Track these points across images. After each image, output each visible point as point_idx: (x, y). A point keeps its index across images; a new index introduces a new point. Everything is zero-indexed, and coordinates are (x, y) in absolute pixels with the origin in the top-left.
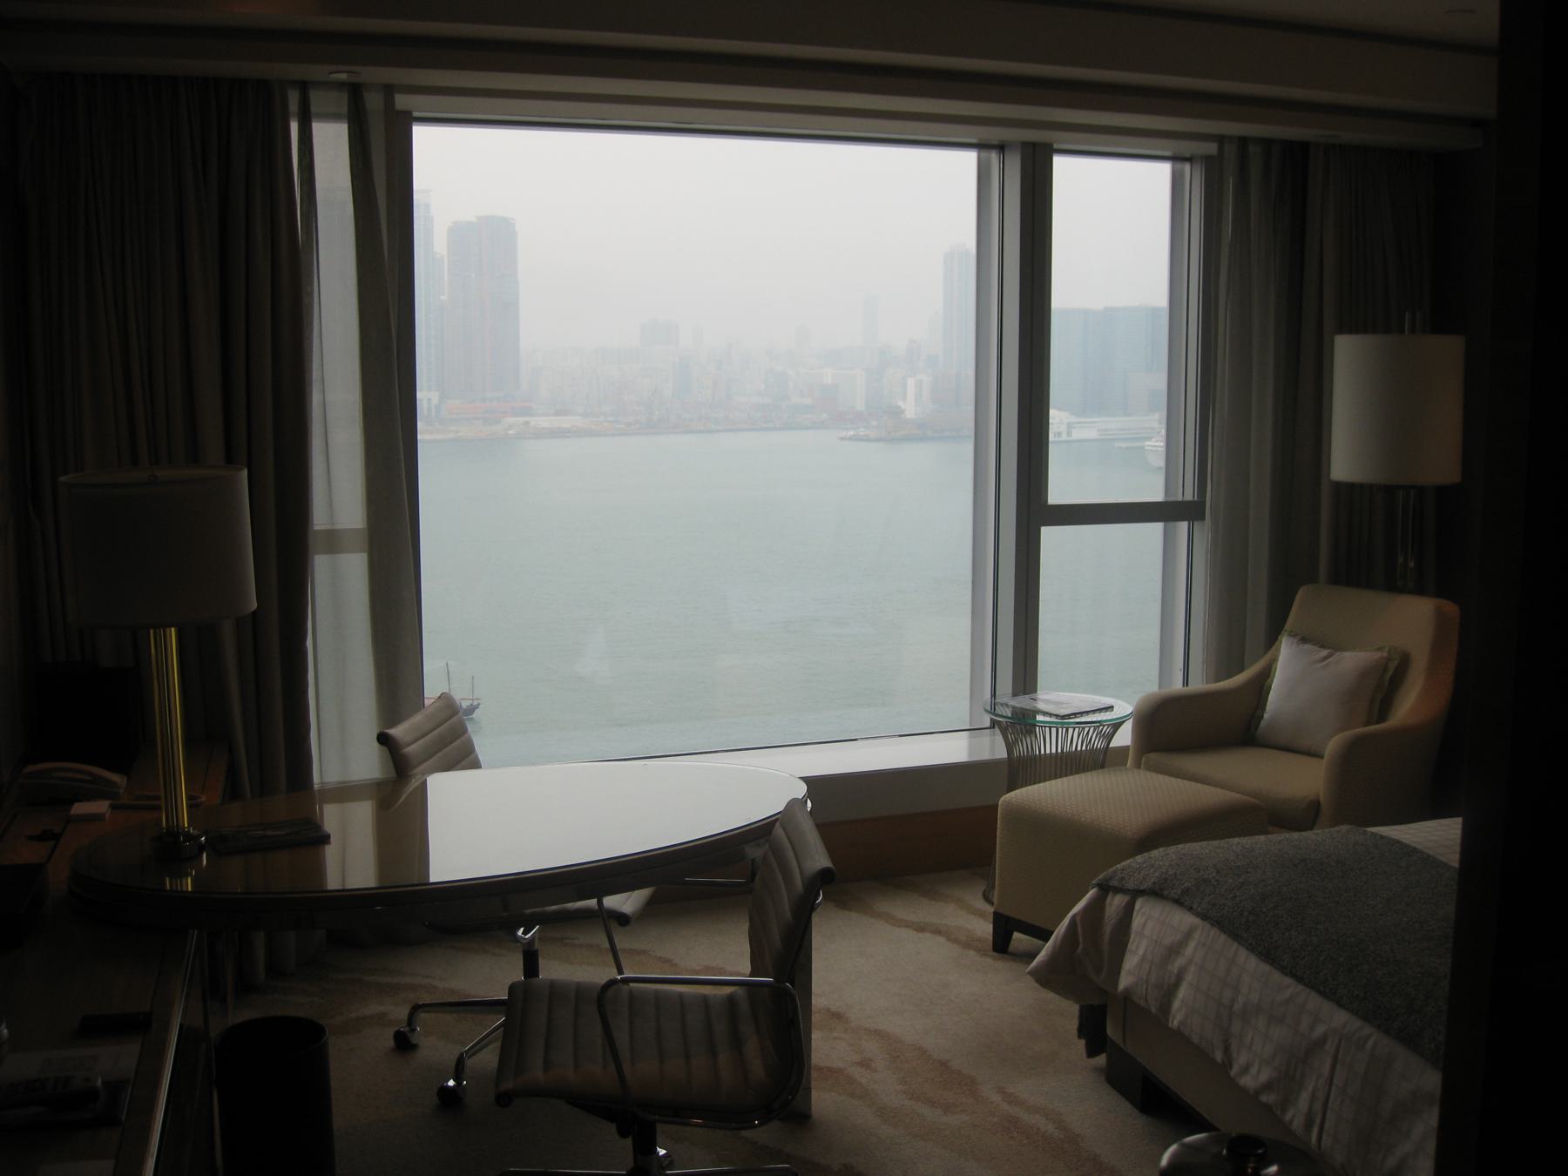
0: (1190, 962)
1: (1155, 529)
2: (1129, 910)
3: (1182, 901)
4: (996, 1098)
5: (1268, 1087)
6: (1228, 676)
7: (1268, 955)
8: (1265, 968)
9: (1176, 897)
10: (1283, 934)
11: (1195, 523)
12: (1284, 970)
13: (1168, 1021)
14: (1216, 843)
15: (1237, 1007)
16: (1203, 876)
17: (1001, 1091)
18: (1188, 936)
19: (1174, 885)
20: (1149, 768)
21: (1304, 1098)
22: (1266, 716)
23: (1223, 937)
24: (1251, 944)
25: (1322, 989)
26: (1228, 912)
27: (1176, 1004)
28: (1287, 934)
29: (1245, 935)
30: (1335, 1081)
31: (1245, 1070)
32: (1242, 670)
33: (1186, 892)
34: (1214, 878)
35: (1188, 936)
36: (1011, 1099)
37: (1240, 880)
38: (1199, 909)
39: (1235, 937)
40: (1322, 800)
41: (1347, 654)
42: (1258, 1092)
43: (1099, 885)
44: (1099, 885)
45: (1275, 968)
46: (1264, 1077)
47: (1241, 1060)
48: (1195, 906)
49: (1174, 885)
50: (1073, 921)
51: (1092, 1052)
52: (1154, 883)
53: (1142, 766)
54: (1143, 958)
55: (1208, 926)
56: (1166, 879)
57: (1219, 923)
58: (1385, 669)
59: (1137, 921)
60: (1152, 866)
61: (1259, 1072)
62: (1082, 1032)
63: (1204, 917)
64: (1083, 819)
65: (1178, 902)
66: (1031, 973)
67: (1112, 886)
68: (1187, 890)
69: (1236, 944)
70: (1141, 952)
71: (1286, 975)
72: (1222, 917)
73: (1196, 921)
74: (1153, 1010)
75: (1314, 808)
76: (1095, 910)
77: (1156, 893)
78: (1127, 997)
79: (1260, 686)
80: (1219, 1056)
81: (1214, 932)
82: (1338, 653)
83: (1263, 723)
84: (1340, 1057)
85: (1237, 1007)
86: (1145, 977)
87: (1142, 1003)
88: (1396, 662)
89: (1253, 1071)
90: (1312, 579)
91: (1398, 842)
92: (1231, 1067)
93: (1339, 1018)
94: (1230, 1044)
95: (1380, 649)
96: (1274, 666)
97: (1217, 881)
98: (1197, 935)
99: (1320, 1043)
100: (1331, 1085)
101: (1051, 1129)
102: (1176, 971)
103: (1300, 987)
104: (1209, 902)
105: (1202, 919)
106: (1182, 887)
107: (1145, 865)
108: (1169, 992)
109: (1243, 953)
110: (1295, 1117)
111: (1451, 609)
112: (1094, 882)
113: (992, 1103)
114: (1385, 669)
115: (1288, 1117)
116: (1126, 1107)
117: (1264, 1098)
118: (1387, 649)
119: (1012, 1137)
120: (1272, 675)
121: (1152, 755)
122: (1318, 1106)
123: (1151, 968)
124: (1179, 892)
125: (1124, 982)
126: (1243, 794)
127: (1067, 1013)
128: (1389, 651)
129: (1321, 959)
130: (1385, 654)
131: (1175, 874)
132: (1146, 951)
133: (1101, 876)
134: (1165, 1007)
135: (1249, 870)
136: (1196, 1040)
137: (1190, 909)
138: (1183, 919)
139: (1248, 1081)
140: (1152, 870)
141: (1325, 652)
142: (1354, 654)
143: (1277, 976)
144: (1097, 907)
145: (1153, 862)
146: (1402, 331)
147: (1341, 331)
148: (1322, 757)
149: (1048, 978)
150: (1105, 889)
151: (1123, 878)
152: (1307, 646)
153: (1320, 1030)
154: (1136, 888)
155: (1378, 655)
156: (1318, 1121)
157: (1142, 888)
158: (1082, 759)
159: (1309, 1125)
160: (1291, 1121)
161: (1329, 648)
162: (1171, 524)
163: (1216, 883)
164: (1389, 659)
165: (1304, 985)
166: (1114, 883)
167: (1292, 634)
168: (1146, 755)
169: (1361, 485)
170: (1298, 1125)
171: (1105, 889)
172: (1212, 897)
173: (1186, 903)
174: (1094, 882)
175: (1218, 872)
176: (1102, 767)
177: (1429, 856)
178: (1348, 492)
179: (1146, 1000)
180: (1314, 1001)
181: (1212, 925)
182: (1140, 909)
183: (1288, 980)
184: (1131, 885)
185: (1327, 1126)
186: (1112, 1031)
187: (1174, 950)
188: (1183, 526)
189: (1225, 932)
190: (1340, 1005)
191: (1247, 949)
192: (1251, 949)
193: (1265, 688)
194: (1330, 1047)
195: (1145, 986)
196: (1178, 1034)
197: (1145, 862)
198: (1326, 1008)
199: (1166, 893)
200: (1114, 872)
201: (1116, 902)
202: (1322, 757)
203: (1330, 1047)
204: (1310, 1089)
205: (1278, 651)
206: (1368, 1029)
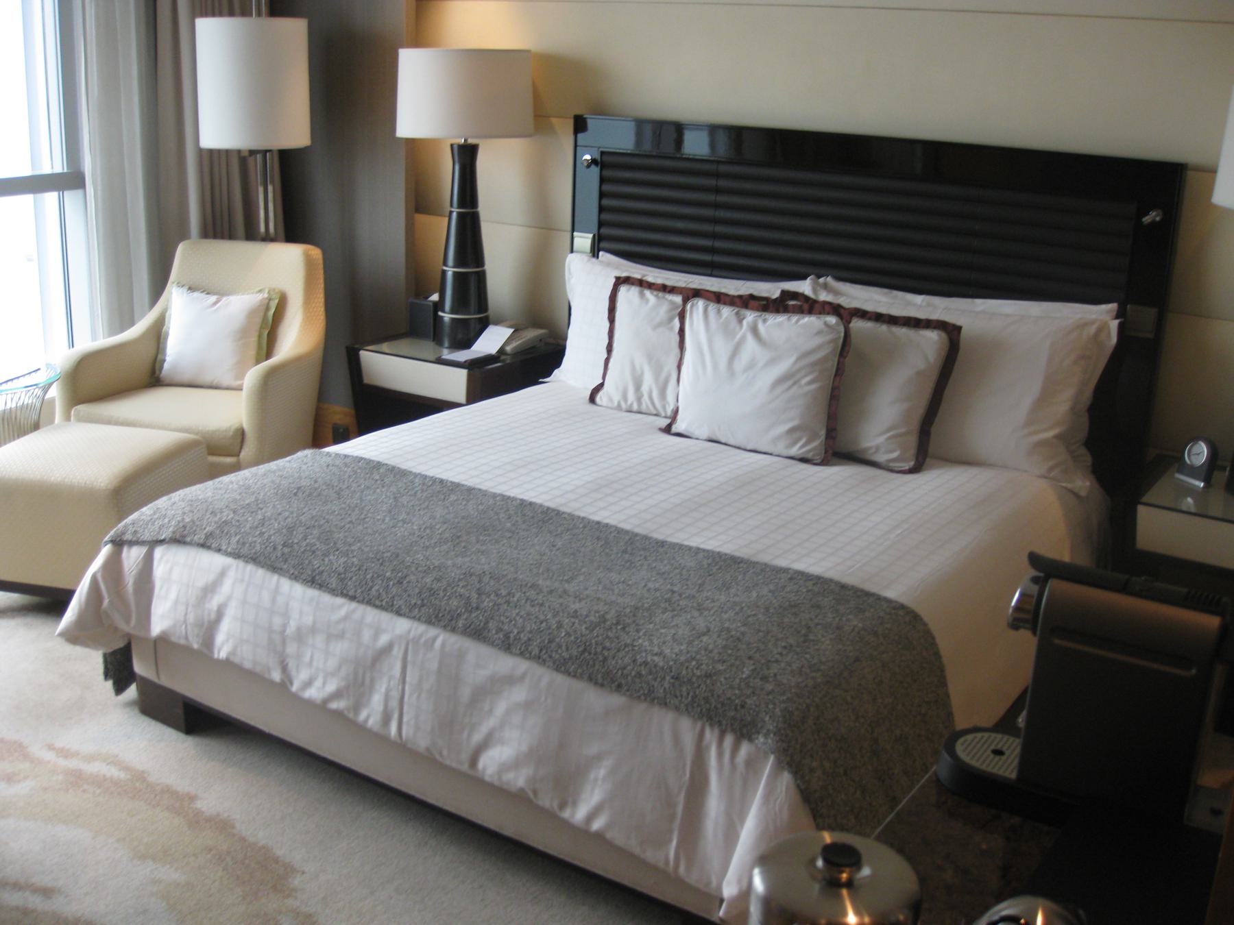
0: (229, 598)
1: (27, 199)
2: (148, 560)
3: (209, 544)
4: (49, 756)
5: (337, 695)
6: (122, 330)
7: (314, 581)
8: (312, 593)
9: (201, 541)
10: (323, 560)
11: (66, 193)
12: (333, 592)
13: (212, 652)
14: (210, 483)
15: (290, 630)
16: (220, 519)
17: (51, 747)
18: (222, 574)
19: (195, 531)
20: (81, 419)
21: (377, 701)
22: (168, 359)
23: (261, 572)
24: (293, 574)
25: (378, 603)
26: (261, 548)
27: (220, 638)
28: (326, 559)
29: (285, 567)
30: (408, 679)
31: (308, 684)
32: (132, 324)
33: (210, 535)
34: (233, 518)
35: (222, 574)
36: (65, 753)
37: (260, 517)
38: (229, 550)
39: (274, 568)
40: (245, 426)
41: (233, 298)
42: (326, 701)
43: (113, 541)
44: (113, 541)
45: (325, 591)
46: (331, 687)
47: (299, 678)
48: (224, 548)
49: (195, 531)
50: (94, 580)
51: (120, 688)
52: (174, 532)
53: (72, 418)
54: (176, 602)
55: (241, 564)
56: (184, 527)
57: (254, 559)
58: (268, 308)
59: (159, 570)
60: (165, 516)
61: (324, 683)
62: (107, 675)
63: (236, 555)
64: (53, 478)
65: (204, 546)
66: (62, 635)
67: (126, 541)
68: (211, 534)
69: (276, 577)
70: (173, 596)
71: (337, 596)
72: (255, 553)
73: (229, 561)
74: (196, 646)
75: (241, 434)
76: (113, 567)
77: (178, 540)
78: (163, 641)
79: (158, 334)
80: (276, 676)
81: (250, 567)
82: (225, 298)
83: (166, 366)
84: (409, 658)
85: (290, 630)
86: (182, 619)
87: (182, 642)
88: (277, 301)
89: (318, 683)
90: (184, 235)
91: (362, 459)
92: (292, 684)
93: (402, 626)
94: (287, 664)
95: (260, 291)
96: (167, 314)
97: (238, 521)
98: (232, 574)
99: (388, 648)
100: (404, 682)
101: (113, 772)
102: (215, 608)
103: (354, 605)
104: (238, 542)
105: (235, 558)
106: (205, 532)
107: (156, 516)
108: (209, 630)
109: (286, 584)
110: (371, 714)
111: (316, 252)
112: (106, 539)
113: (49, 762)
114: (268, 308)
115: (362, 716)
116: (181, 736)
117: (334, 705)
118: (267, 291)
119: (84, 791)
120: (166, 323)
121: (81, 407)
122: (394, 704)
123: (187, 609)
124: (203, 537)
125: (157, 627)
126: (190, 433)
127: (93, 661)
128: (269, 292)
129: (368, 577)
130: (266, 295)
131: (193, 521)
132: (178, 595)
133: (112, 533)
134: (209, 640)
135: (261, 506)
136: (248, 665)
137: (219, 550)
138: (211, 562)
139: (313, 693)
140: (166, 520)
141: (213, 298)
142: (239, 297)
143: (327, 598)
144: (114, 564)
145: (164, 513)
146: (251, 15)
147: (205, 14)
148: (242, 390)
149: (74, 636)
150: (119, 543)
151: (135, 532)
152: (196, 294)
153: (384, 639)
154: (155, 539)
155: (260, 297)
156: (396, 716)
157: (163, 537)
158: (22, 423)
159: (386, 719)
160: (366, 720)
161: (214, 294)
162: (40, 196)
163: (237, 524)
164: (270, 299)
165: (358, 602)
166: (128, 537)
167: (180, 285)
168: (74, 408)
169: (219, 151)
170: (373, 722)
171: (119, 543)
172: (238, 537)
173: (213, 546)
174: (106, 539)
175: (234, 512)
176: (36, 427)
177: (394, 468)
178: (212, 158)
179: (187, 638)
180: (371, 615)
181: (247, 562)
182: (161, 558)
183: (339, 601)
184: (147, 536)
185: (405, 719)
186: (139, 668)
187: (209, 590)
188: (51, 198)
189: (263, 567)
190: (399, 613)
191: (290, 578)
192: (294, 578)
193: (162, 337)
194: (397, 652)
195: (184, 627)
196: (228, 664)
197: (155, 513)
198: (385, 618)
199: (188, 539)
200: (125, 526)
201: (132, 557)
202: (242, 390)
203: (397, 652)
204: (383, 690)
205: (168, 300)
206: (433, 631)
